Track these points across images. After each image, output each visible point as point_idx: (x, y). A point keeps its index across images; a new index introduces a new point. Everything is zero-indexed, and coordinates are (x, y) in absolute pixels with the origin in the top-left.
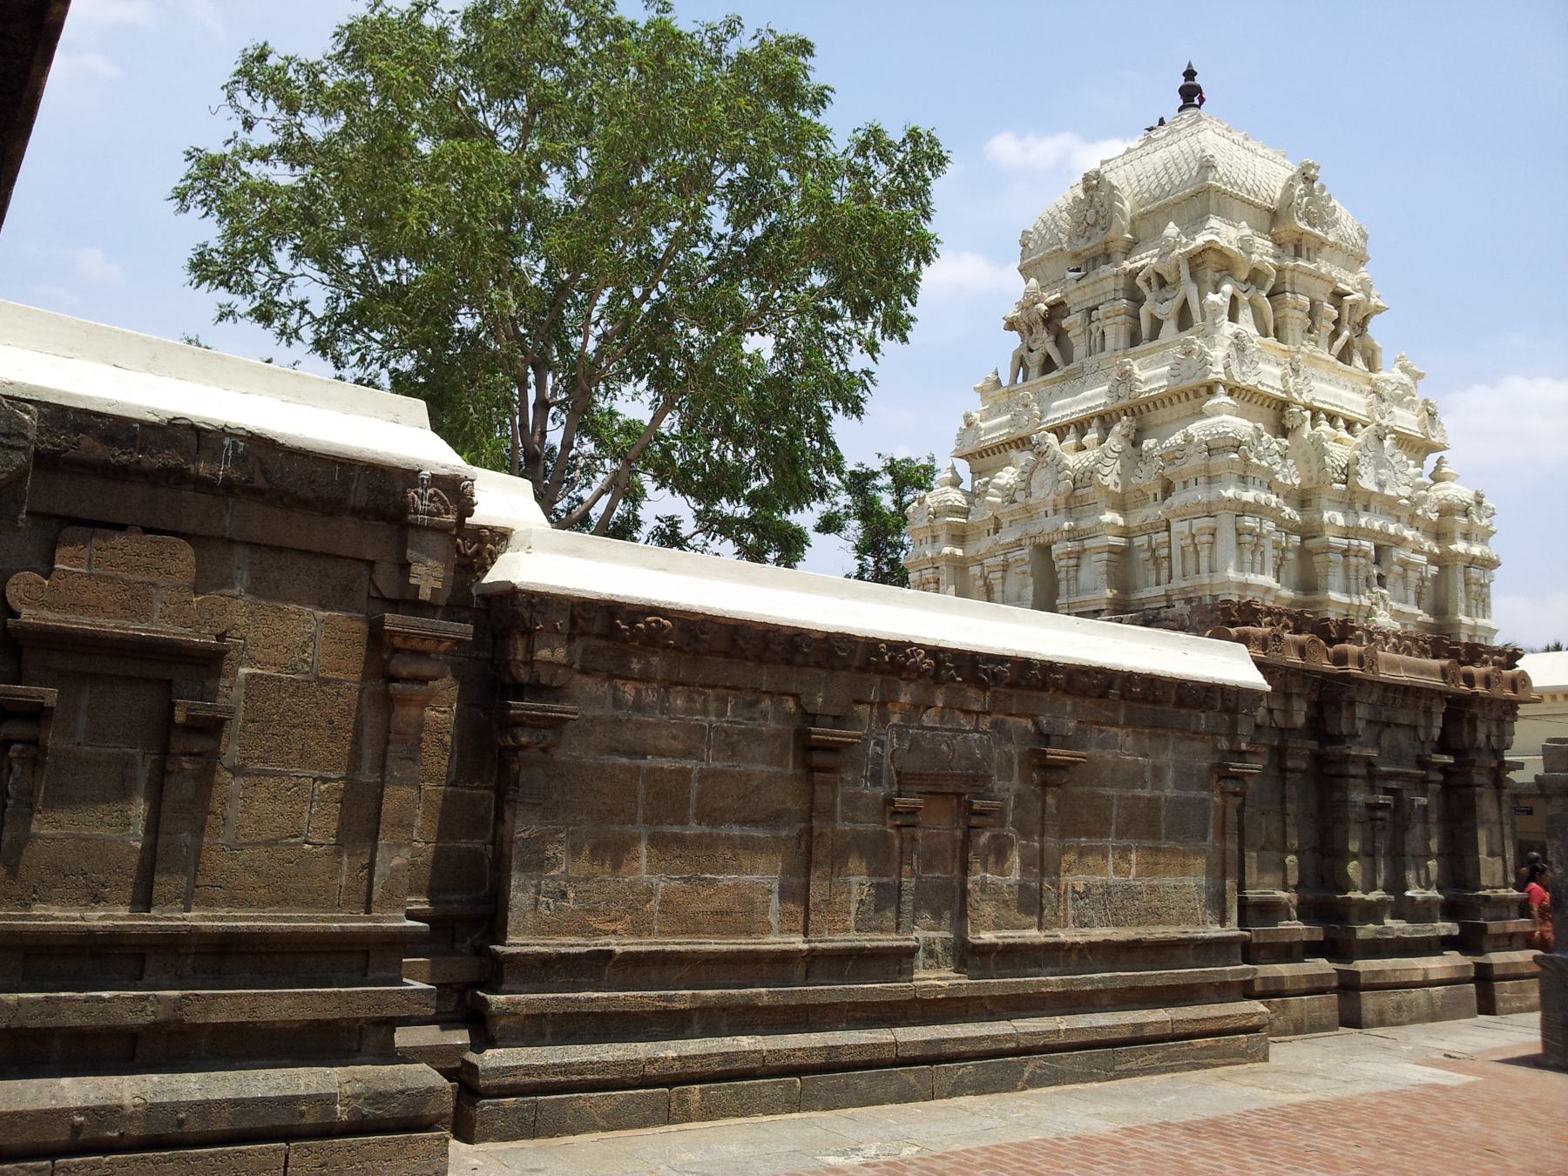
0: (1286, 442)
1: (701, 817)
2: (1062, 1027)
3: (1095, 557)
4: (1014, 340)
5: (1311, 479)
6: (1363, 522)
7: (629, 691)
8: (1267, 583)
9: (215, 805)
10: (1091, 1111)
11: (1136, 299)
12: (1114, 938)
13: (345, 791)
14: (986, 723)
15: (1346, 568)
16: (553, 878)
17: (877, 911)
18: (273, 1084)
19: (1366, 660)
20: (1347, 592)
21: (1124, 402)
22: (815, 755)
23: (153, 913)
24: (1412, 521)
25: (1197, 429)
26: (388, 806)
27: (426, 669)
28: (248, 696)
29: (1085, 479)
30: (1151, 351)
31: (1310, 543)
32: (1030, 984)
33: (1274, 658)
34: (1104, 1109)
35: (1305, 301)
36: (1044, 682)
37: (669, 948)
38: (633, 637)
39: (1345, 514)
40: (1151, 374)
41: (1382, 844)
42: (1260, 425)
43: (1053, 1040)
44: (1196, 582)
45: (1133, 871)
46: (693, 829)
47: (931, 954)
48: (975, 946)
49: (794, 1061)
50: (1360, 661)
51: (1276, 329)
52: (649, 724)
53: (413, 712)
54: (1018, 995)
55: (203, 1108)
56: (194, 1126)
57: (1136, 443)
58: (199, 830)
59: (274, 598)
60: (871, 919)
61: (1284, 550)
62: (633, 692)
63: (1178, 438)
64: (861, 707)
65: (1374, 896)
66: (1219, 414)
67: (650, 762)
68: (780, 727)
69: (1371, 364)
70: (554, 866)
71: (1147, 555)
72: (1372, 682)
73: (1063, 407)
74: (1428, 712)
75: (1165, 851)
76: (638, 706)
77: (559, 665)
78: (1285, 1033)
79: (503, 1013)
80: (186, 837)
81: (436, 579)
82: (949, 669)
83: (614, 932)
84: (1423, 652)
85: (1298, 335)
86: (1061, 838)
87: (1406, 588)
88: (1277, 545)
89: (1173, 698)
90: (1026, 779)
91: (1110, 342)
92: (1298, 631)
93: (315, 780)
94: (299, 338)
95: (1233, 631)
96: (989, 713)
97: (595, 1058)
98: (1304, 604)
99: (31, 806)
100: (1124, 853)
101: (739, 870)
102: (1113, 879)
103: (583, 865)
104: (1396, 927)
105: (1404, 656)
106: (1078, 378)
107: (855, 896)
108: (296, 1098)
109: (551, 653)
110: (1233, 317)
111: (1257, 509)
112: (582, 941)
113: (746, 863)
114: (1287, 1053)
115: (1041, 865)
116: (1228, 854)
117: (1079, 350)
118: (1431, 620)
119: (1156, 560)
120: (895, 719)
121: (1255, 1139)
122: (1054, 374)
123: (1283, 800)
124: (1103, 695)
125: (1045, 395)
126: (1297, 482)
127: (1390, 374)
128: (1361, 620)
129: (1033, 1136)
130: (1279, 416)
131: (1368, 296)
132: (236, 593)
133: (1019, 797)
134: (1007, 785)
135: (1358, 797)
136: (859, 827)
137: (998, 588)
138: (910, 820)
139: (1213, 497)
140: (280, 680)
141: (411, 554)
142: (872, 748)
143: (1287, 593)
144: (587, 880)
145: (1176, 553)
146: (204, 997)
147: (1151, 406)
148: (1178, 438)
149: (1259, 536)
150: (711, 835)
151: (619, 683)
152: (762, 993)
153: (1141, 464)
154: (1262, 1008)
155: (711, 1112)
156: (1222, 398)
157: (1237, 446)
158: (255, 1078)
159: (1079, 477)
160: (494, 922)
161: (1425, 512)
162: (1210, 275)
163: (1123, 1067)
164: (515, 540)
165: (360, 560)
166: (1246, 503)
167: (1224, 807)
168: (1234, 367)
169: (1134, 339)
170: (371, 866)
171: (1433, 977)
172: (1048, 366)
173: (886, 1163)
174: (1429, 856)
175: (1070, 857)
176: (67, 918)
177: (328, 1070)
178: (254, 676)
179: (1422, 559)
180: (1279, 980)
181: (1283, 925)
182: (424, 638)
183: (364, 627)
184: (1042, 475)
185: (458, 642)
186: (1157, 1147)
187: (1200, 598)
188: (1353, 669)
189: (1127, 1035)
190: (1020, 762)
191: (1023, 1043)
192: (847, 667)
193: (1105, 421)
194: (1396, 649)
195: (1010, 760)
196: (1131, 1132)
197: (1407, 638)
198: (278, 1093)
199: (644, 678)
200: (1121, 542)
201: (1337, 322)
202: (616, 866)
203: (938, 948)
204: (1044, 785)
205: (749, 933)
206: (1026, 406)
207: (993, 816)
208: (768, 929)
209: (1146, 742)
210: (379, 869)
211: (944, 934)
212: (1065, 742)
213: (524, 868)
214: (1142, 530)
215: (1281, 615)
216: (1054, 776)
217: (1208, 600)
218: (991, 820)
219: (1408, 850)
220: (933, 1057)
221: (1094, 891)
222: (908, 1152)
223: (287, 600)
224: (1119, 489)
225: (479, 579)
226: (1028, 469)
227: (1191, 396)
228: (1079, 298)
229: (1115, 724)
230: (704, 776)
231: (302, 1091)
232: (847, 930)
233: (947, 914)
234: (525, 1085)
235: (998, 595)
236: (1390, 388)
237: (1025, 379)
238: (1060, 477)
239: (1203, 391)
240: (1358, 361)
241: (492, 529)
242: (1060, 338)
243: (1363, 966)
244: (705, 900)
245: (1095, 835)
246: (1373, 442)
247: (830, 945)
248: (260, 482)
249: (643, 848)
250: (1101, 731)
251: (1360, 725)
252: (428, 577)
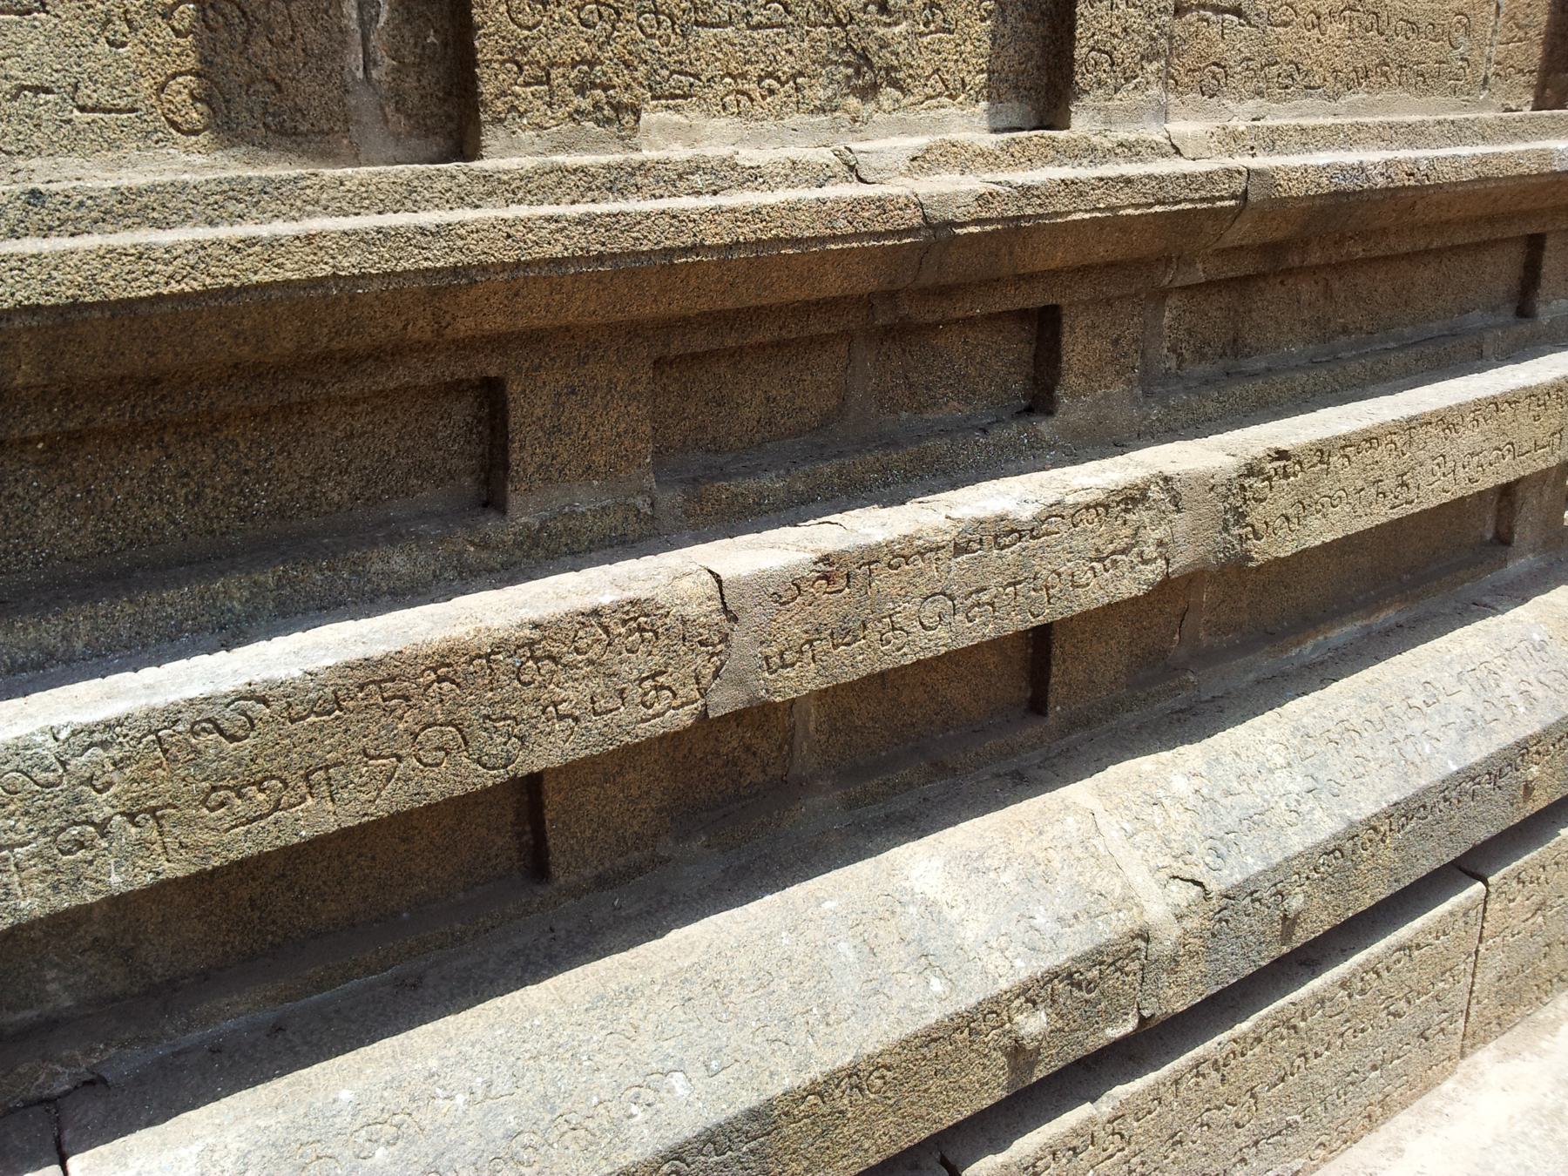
23: (1082, 124)
176: (795, 171)
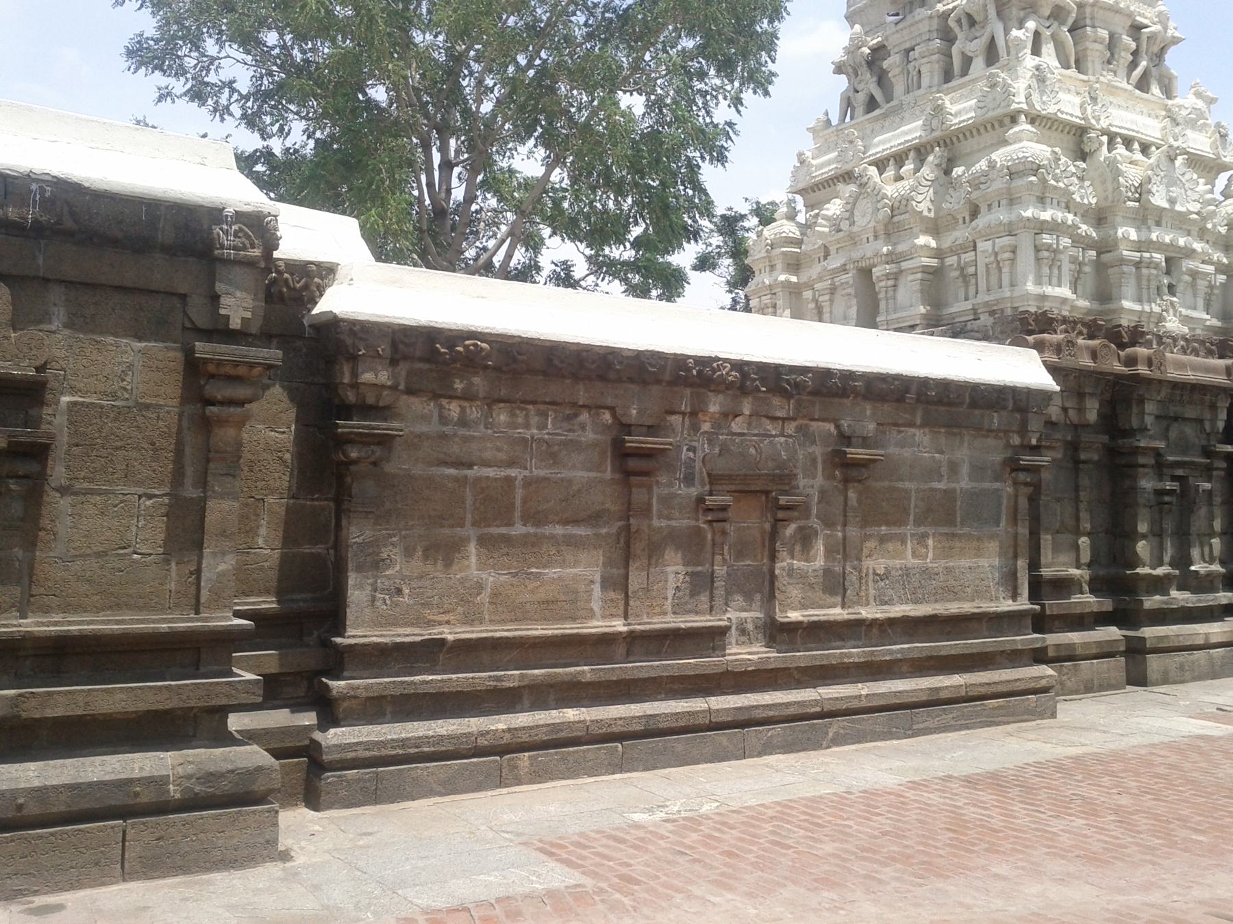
0: (1084, 165)
1: (527, 518)
2: (863, 693)
3: (910, 278)
4: (842, 82)
5: (1106, 199)
6: (1154, 236)
7: (454, 409)
8: (1062, 294)
9: (45, 522)
10: (883, 766)
11: (949, 38)
12: (912, 614)
13: (170, 506)
14: (790, 428)
15: (1139, 278)
16: (388, 577)
17: (692, 595)
18: (109, 769)
19: (1155, 362)
20: (1139, 300)
21: (937, 134)
22: (632, 461)
24: (1202, 234)
25: (1000, 156)
26: (212, 518)
27: (241, 392)
28: (71, 423)
29: (901, 206)
30: (961, 86)
31: (1106, 257)
32: (834, 655)
33: (1067, 361)
34: (896, 764)
35: (1104, 34)
36: (844, 389)
37: (498, 635)
38: (454, 361)
39: (1138, 229)
40: (960, 108)
41: (1169, 525)
42: (1057, 149)
43: (855, 704)
44: (998, 296)
45: (930, 555)
46: (519, 529)
47: (743, 631)
48: (782, 624)
49: (615, 729)
50: (1150, 362)
51: (1077, 61)
52: (474, 437)
53: (231, 432)
54: (822, 666)
55: (41, 793)
56: (33, 809)
57: (947, 172)
58: (31, 544)
59: (92, 331)
60: (686, 603)
61: (1080, 264)
62: (458, 410)
63: (982, 165)
65: (1160, 571)
66: (1021, 141)
67: (476, 472)
68: (599, 437)
69: (1168, 92)
70: (388, 567)
71: (957, 273)
72: (1160, 382)
73: (883, 142)
74: (1213, 407)
75: (959, 536)
76: (463, 422)
77: (383, 387)
78: (1077, 692)
79: (344, 697)
80: (18, 552)
81: (246, 309)
82: (755, 380)
83: (448, 622)
84: (1210, 353)
85: (1098, 66)
86: (863, 526)
87: (1195, 295)
88: (1074, 260)
89: (968, 400)
90: (829, 477)
91: (925, 81)
92: (1091, 337)
93: (140, 497)
94: (231, 114)
95: (1030, 339)
96: (794, 419)
97: (431, 733)
98: (1101, 313)
100: (924, 536)
101: (563, 564)
102: (912, 562)
103: (417, 564)
104: (1180, 597)
105: (1192, 358)
106: (897, 114)
107: (672, 583)
108: (129, 782)
109: (375, 375)
110: (1036, 51)
111: (1054, 227)
112: (417, 631)
113: (569, 558)
114: (1071, 710)
115: (843, 551)
116: (1020, 537)
117: (899, 88)
118: (1219, 324)
119: (964, 276)
120: (706, 427)
121: (1027, 789)
122: (877, 112)
123: (1077, 489)
124: (900, 399)
125: (868, 131)
126: (1094, 201)
127: (1185, 101)
128: (1152, 326)
129: (825, 790)
130: (1078, 139)
131: (1166, 28)
132: (53, 328)
133: (822, 492)
134: (811, 482)
135: (1147, 484)
136: (673, 523)
137: (826, 309)
138: (721, 515)
139: (1013, 217)
140: (102, 407)
141: (220, 287)
142: (685, 454)
143: (1083, 303)
144: (420, 577)
145: (981, 270)
146: (38, 694)
147: (961, 136)
148: (982, 165)
149: (1056, 251)
150: (536, 535)
151: (444, 402)
152: (585, 671)
153: (951, 191)
154: (1050, 672)
155: (539, 775)
156: (1024, 126)
157: (1035, 169)
158: (92, 764)
159: (896, 205)
160: (335, 618)
161: (1214, 226)
162: (1015, 12)
163: (921, 726)
164: (340, 273)
165: (172, 294)
166: (1045, 221)
167: (1016, 496)
168: (1035, 97)
169: (948, 76)
171: (1214, 640)
172: (872, 104)
173: (685, 819)
174: (1212, 534)
175: (871, 544)
177: (162, 755)
178: (75, 404)
179: (1210, 269)
180: (1071, 646)
181: (1076, 598)
182: (236, 364)
184: (864, 206)
185: (269, 367)
186: (935, 798)
187: (1002, 310)
188: (1142, 370)
189: (924, 698)
190: (824, 462)
191: (827, 707)
192: (659, 382)
193: (920, 152)
194: (1184, 351)
195: (814, 461)
196: (914, 785)
197: (1196, 341)
198: (113, 777)
199: (468, 396)
200: (933, 262)
201: (1135, 53)
202: (448, 564)
203: (750, 627)
204: (846, 481)
205: (574, 619)
206: (851, 142)
207: (801, 509)
208: (591, 615)
209: (943, 440)
210: (206, 575)
211: (753, 615)
212: (865, 442)
213: (359, 569)
214: (953, 251)
215: (1075, 323)
216: (854, 473)
217: (1009, 312)
218: (796, 514)
219: (1193, 529)
220: (744, 721)
221: (893, 573)
222: (708, 808)
223: (102, 333)
224: (932, 215)
225: (310, 310)
226: (851, 200)
227: (996, 125)
228: (898, 41)
229: (911, 425)
230: (528, 483)
231: (136, 774)
232: (665, 614)
233: (758, 596)
234: (366, 759)
235: (826, 316)
236: (1184, 113)
237: (852, 118)
238: (880, 205)
239: (1007, 121)
240: (1155, 89)
241: (318, 265)
242: (882, 79)
243: (1149, 632)
244: (532, 592)
245: (894, 524)
246: (1164, 163)
247: (648, 627)
248: (69, 224)
249: (472, 548)
250: (900, 432)
251: (1149, 420)
252: (238, 306)
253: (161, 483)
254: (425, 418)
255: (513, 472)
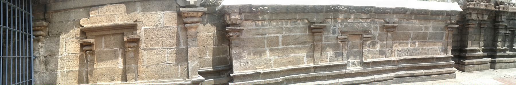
58: (137, 63)
64: (328, 20)
76: (263, 25)
99: (93, 62)
170: (188, 67)
183: (176, 14)
253: (173, 46)
254: (252, 26)
255: (278, 35)
